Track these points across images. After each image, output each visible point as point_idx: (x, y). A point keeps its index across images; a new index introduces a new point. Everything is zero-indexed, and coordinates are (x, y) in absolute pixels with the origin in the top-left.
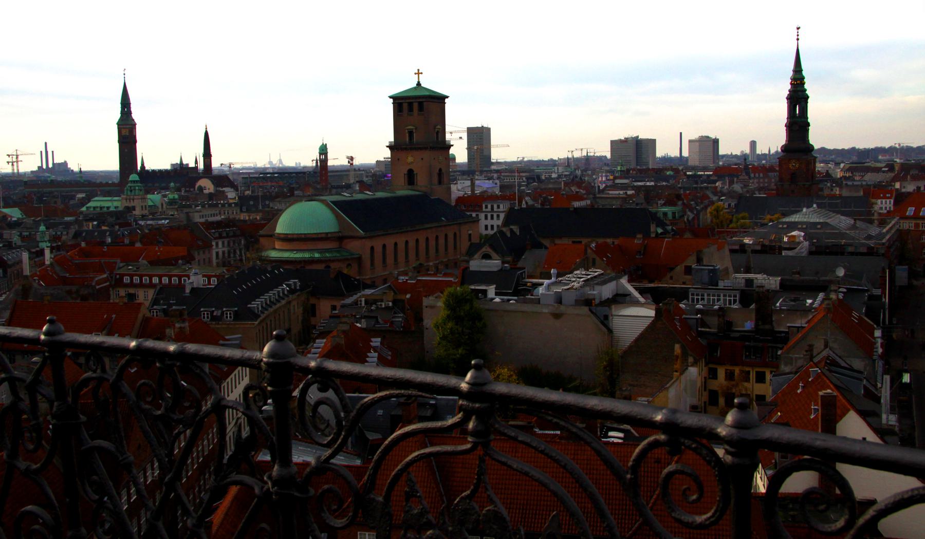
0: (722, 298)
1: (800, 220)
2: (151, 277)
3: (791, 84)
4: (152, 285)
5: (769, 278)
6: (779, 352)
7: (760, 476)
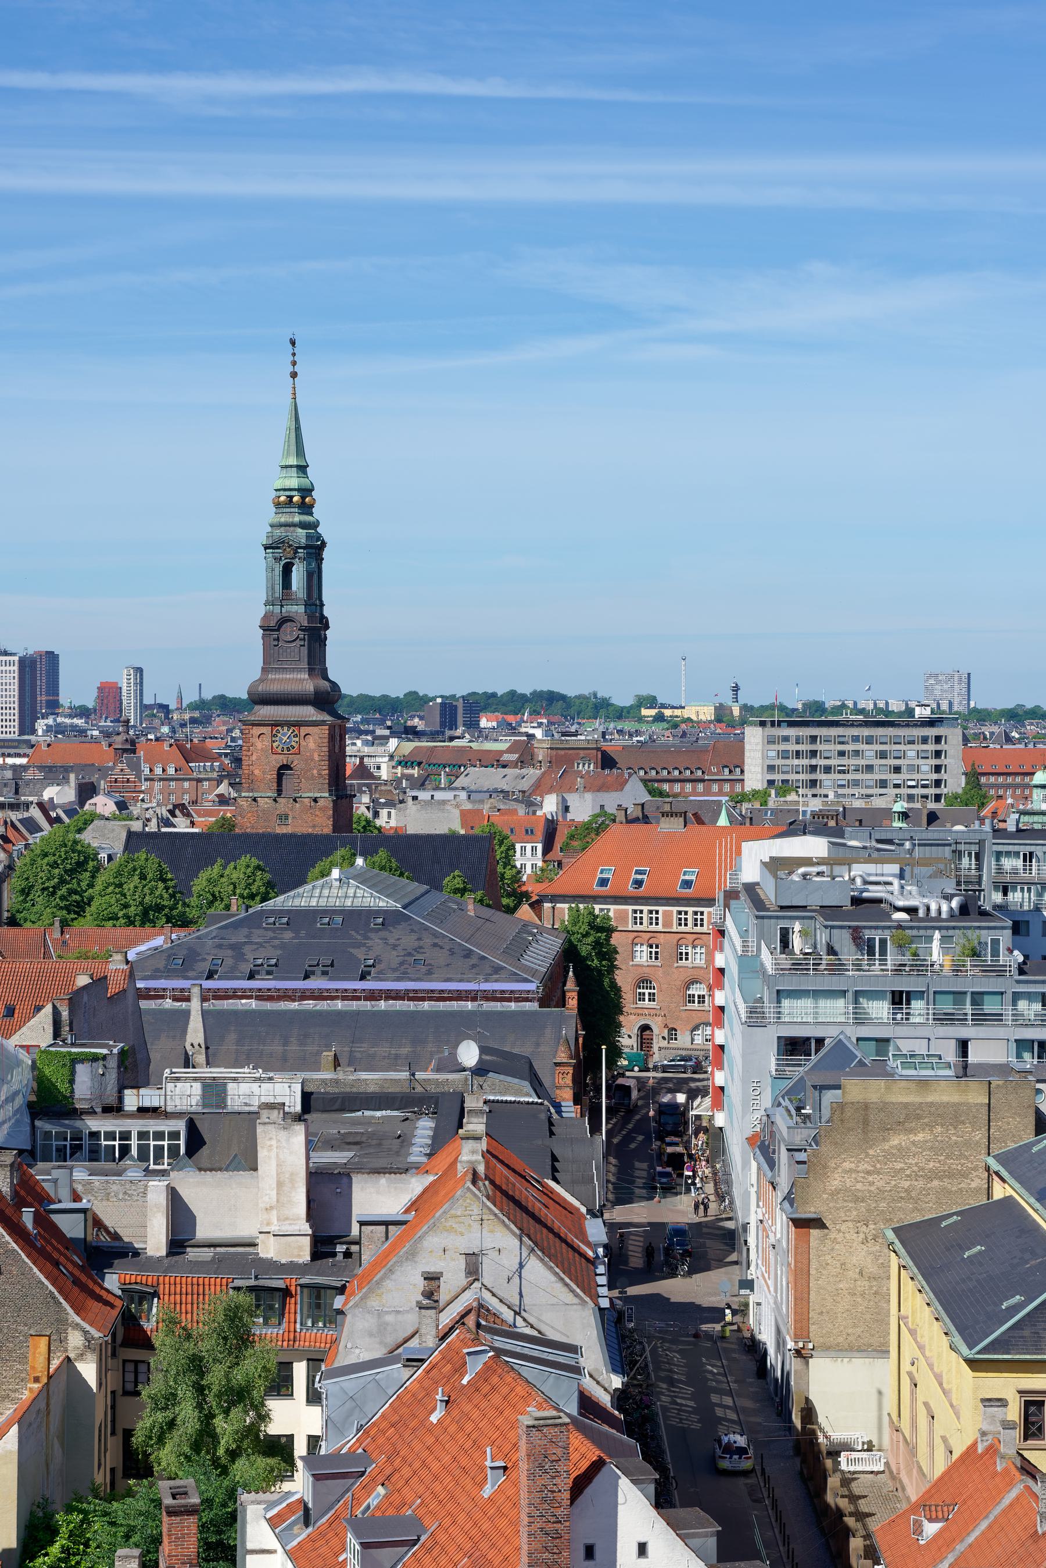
1: (323, 902)
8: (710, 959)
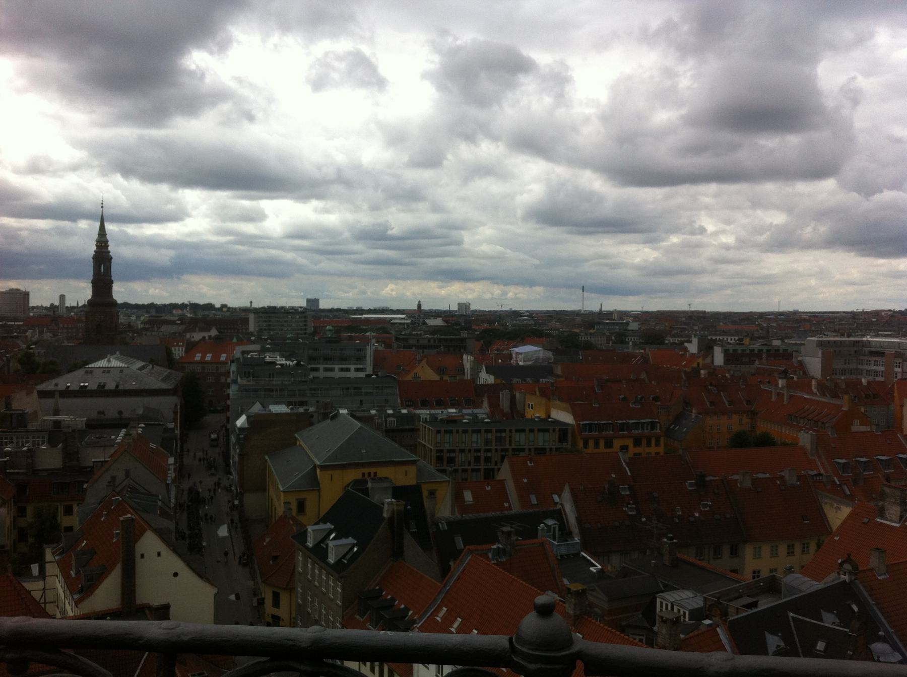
0: (30, 440)
3: (97, 245)
5: (75, 419)
6: (85, 486)
7: (68, 601)
8: (226, 380)
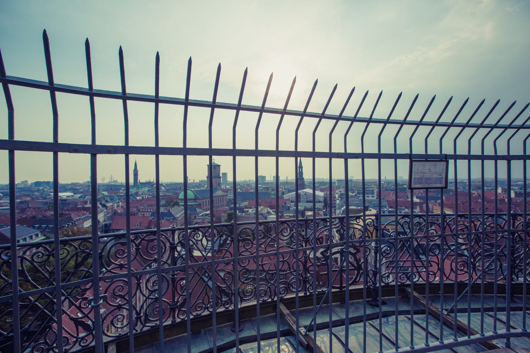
2: (148, 209)
4: (150, 212)
